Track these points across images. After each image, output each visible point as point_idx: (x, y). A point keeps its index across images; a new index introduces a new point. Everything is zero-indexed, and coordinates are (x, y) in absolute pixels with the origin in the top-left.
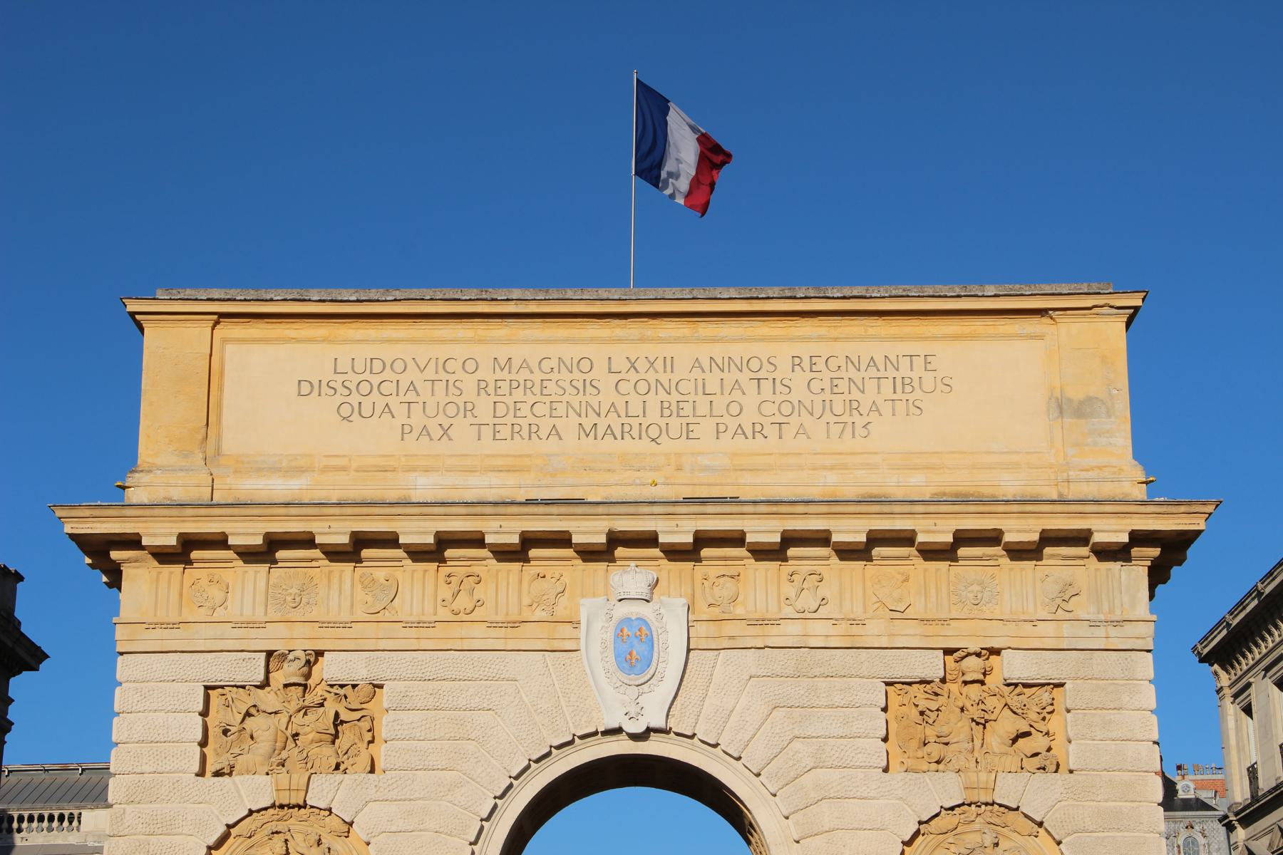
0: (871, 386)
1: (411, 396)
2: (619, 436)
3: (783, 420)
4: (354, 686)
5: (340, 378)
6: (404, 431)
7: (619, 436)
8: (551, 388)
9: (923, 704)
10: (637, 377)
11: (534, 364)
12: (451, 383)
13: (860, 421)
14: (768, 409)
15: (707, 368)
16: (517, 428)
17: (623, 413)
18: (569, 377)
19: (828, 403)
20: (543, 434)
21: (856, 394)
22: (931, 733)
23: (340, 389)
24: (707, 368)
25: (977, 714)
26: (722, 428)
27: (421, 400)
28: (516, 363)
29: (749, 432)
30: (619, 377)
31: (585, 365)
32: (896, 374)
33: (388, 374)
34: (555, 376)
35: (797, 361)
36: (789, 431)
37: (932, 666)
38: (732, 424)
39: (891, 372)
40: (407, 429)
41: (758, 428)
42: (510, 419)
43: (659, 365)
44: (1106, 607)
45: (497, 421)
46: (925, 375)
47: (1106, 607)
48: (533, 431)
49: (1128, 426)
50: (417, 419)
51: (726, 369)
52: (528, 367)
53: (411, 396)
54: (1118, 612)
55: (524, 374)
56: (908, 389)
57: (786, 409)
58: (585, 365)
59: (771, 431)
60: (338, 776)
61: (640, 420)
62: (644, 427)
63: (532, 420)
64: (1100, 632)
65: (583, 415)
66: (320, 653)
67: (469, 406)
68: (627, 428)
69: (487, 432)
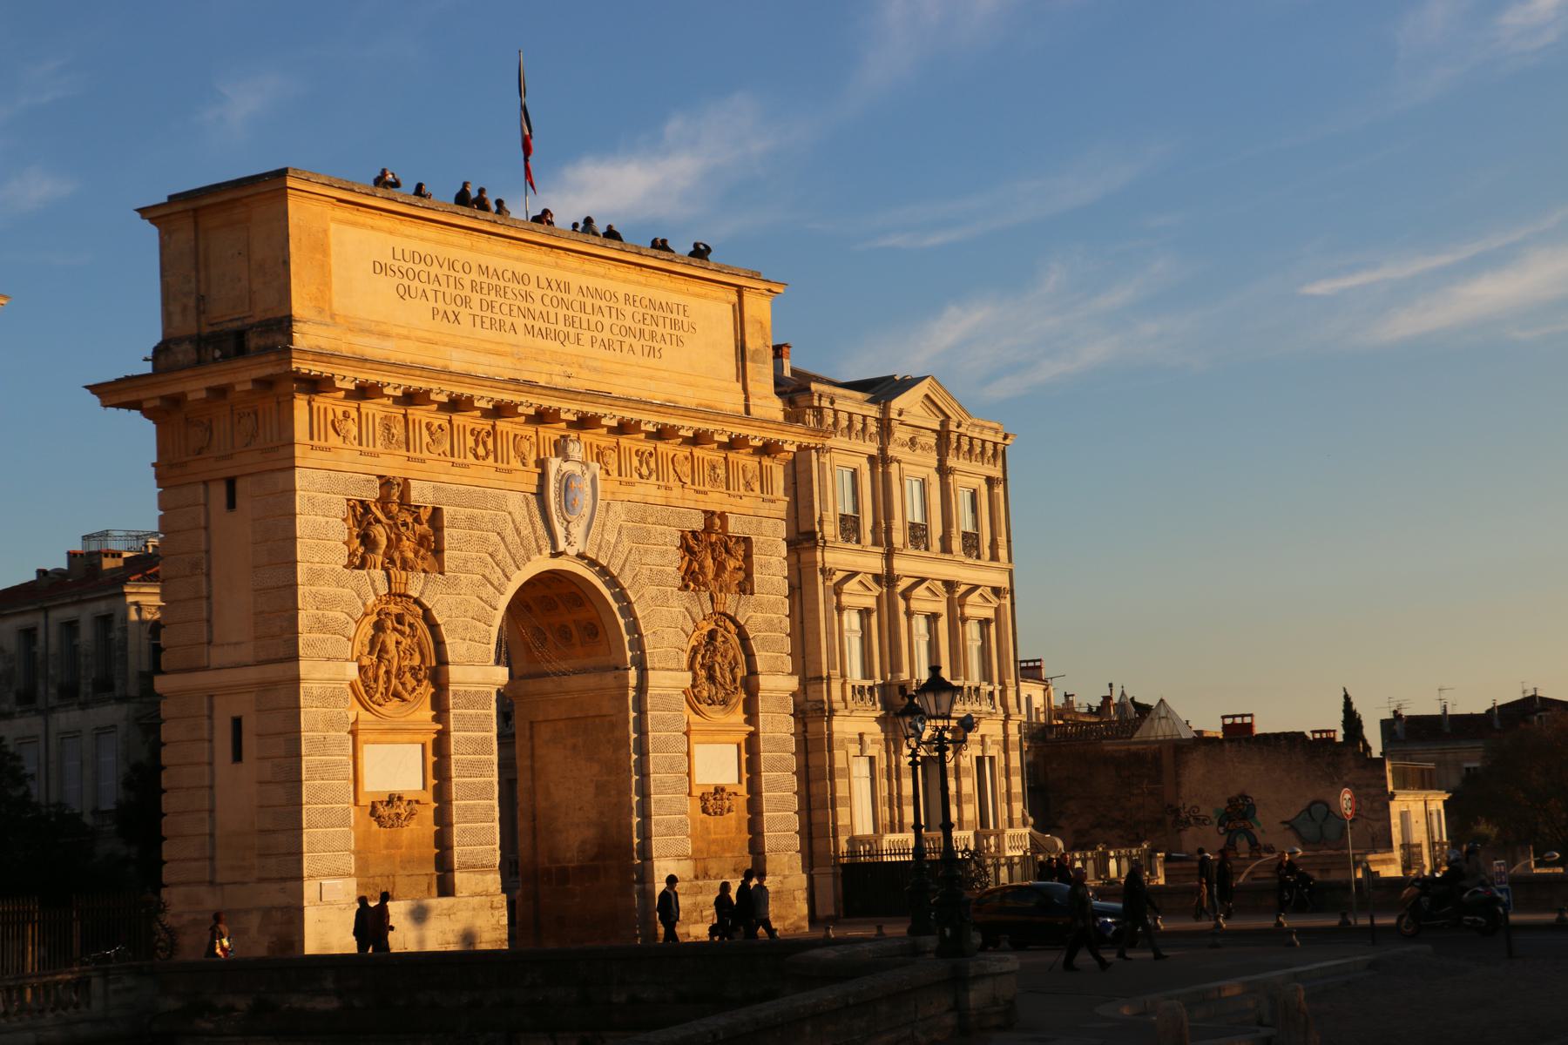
1: (436, 287)
5: (397, 264)
8: (510, 294)
14: (616, 330)
16: (493, 322)
20: (507, 328)
21: (654, 327)
28: (491, 271)
33: (422, 266)
34: (510, 284)
40: (436, 312)
45: (483, 314)
53: (436, 287)
55: (494, 281)
56: (677, 328)
60: (423, 575)
63: (502, 317)
64: (767, 505)
67: (468, 301)
69: (478, 320)
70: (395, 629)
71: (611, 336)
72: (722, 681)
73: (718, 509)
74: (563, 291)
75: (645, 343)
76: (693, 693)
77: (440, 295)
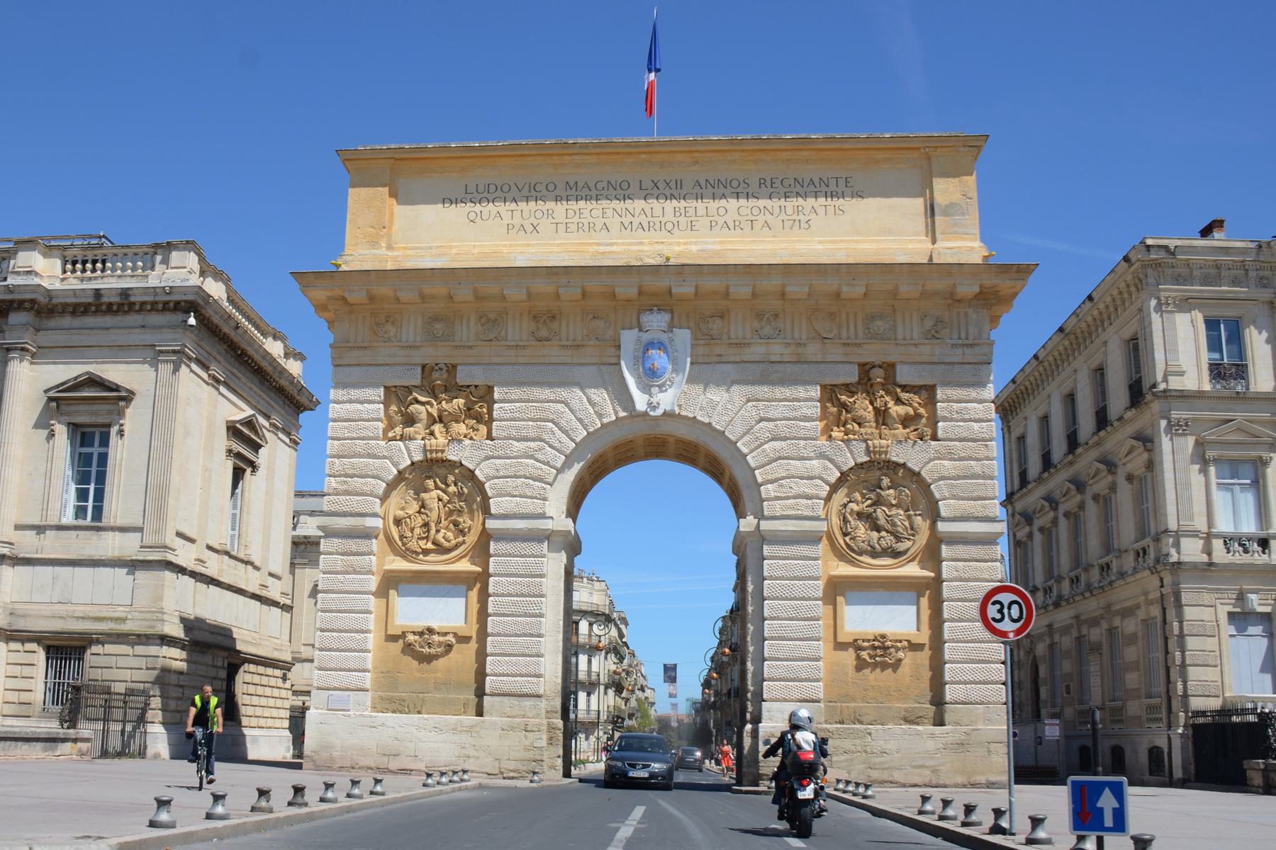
2: (646, 229)
3: (753, 218)
4: (476, 386)
7: (646, 229)
9: (843, 398)
10: (659, 192)
11: (592, 185)
15: (704, 187)
16: (580, 225)
17: (649, 215)
18: (615, 193)
19: (783, 208)
20: (597, 228)
22: (849, 415)
24: (704, 187)
25: (878, 403)
26: (714, 224)
27: (519, 208)
28: (580, 185)
29: (731, 226)
30: (647, 192)
31: (625, 185)
35: (762, 181)
36: (757, 225)
38: (721, 221)
40: (511, 227)
41: (737, 223)
42: (576, 219)
43: (673, 184)
44: (963, 336)
45: (567, 221)
47: (963, 336)
48: (591, 227)
49: (977, 221)
50: (517, 221)
51: (716, 187)
52: (588, 187)
54: (971, 338)
57: (755, 211)
58: (625, 185)
59: (747, 226)
60: (467, 442)
61: (659, 219)
62: (663, 223)
63: (591, 220)
64: (959, 351)
65: (624, 216)
66: (454, 367)
67: (550, 212)
68: (652, 224)
69: (562, 228)
70: (437, 487)
71: (737, 217)
72: (890, 528)
73: (878, 362)
74: (674, 187)
76: (845, 541)
77: (517, 214)
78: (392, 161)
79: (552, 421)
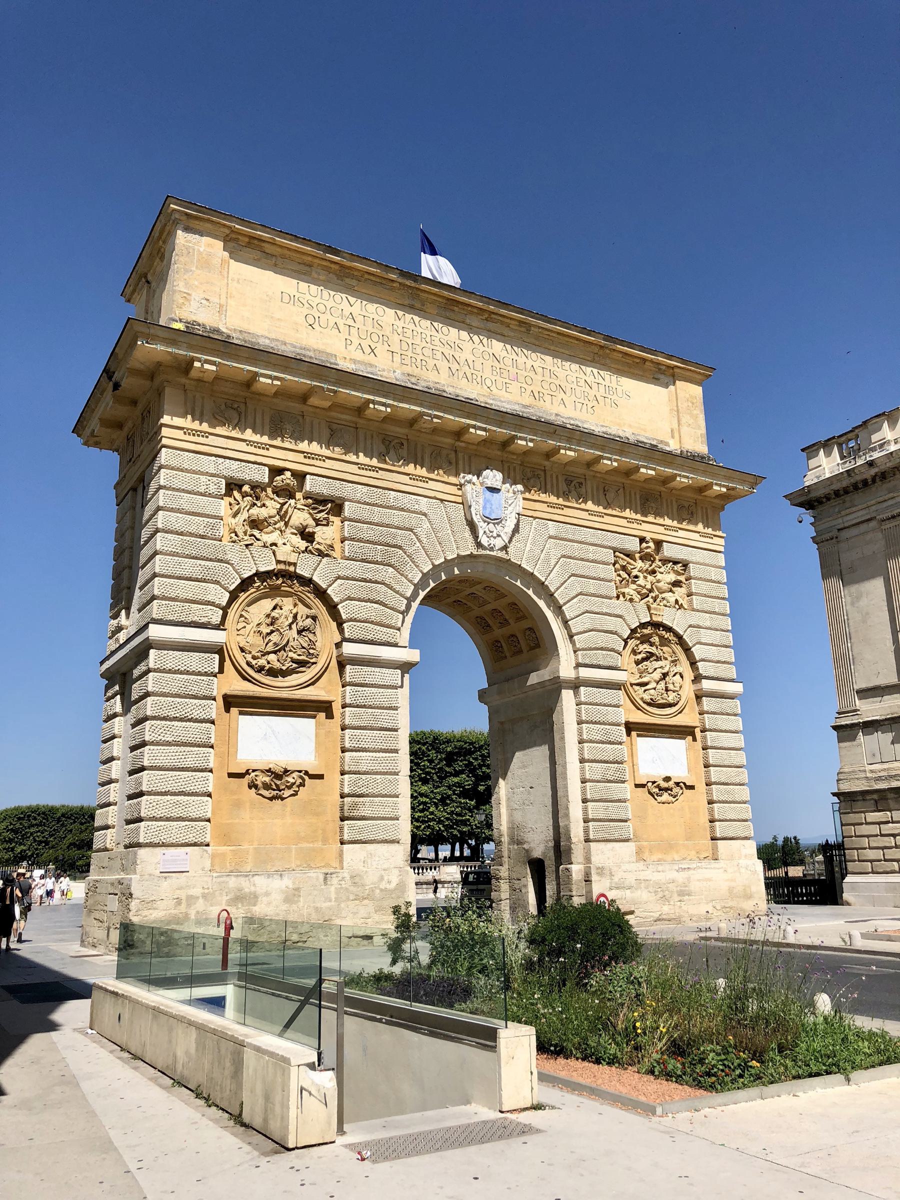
0: (595, 386)
6: (348, 342)
12: (375, 320)
13: (590, 405)
23: (307, 305)
32: (604, 383)
37: (633, 545)
38: (529, 389)
39: (601, 381)
41: (541, 395)
46: (617, 387)
53: (352, 323)
57: (553, 387)
59: (548, 398)
63: (423, 358)
65: (451, 361)
68: (475, 377)
69: (397, 358)
75: (577, 400)
78: (227, 231)
79: (400, 547)
